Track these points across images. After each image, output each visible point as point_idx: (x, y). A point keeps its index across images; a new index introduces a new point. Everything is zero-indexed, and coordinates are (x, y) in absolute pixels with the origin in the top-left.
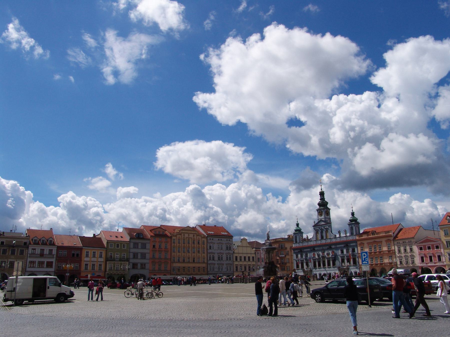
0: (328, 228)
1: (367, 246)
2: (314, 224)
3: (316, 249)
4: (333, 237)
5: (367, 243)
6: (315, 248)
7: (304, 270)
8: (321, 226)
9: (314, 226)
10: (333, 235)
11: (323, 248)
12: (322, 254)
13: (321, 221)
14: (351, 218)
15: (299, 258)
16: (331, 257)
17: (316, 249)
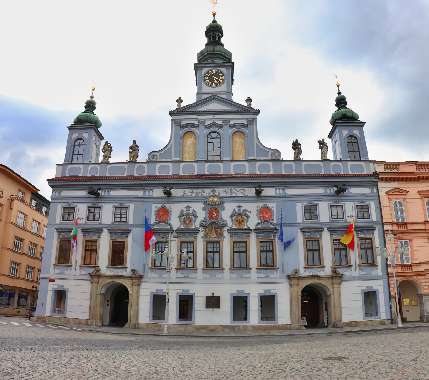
0: (246, 126)
1: (420, 200)
2: (177, 107)
3: (176, 192)
4: (270, 158)
5: (419, 192)
6: (172, 191)
7: (98, 271)
8: (211, 117)
9: (171, 113)
10: (271, 152)
11: (214, 191)
12: (210, 215)
13: (214, 98)
14: (335, 111)
15: (79, 222)
16: (252, 227)
17: (176, 192)
